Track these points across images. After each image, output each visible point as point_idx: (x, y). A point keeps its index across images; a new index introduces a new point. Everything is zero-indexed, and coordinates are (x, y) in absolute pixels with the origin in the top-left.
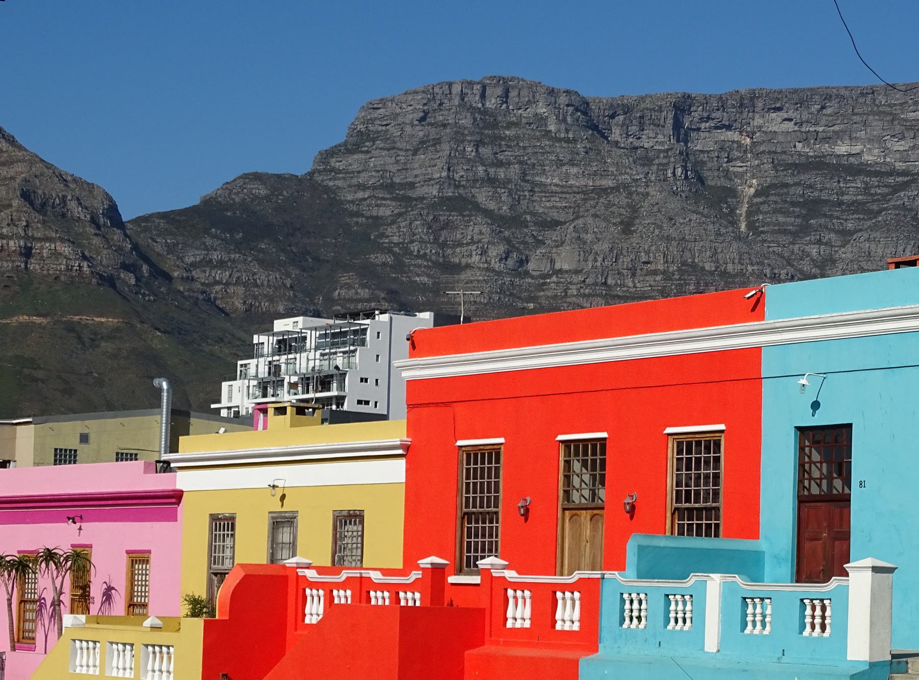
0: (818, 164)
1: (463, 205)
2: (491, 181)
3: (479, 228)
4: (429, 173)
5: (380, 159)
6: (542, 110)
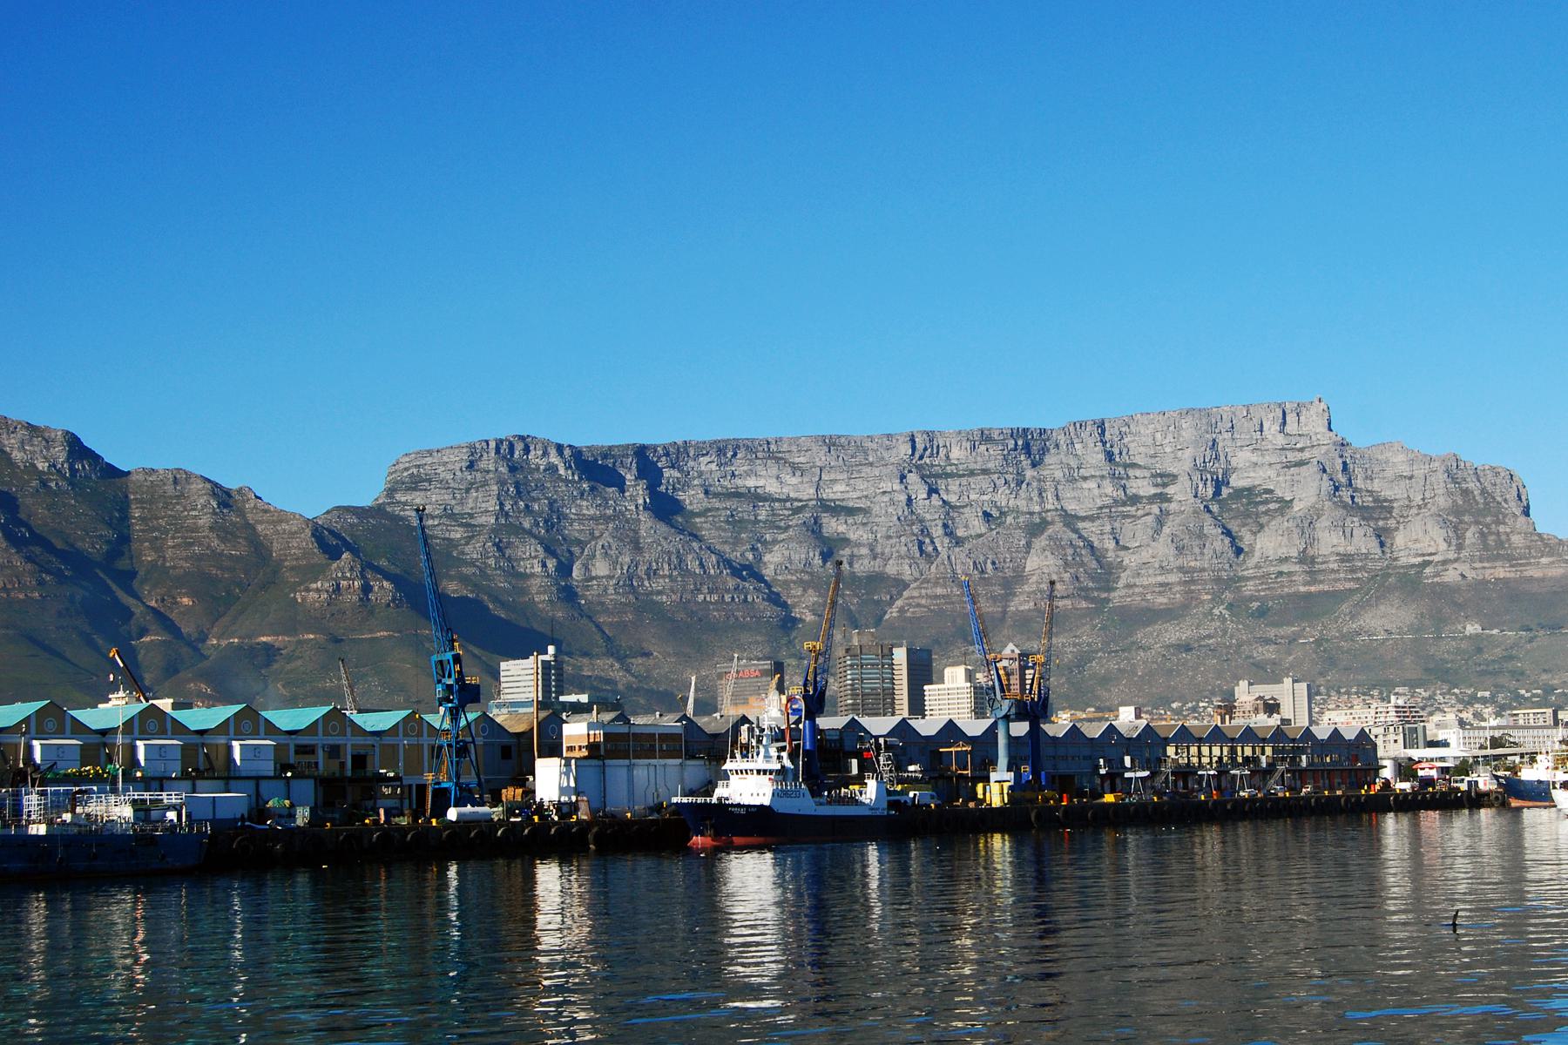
0: (737, 495)
1: (518, 530)
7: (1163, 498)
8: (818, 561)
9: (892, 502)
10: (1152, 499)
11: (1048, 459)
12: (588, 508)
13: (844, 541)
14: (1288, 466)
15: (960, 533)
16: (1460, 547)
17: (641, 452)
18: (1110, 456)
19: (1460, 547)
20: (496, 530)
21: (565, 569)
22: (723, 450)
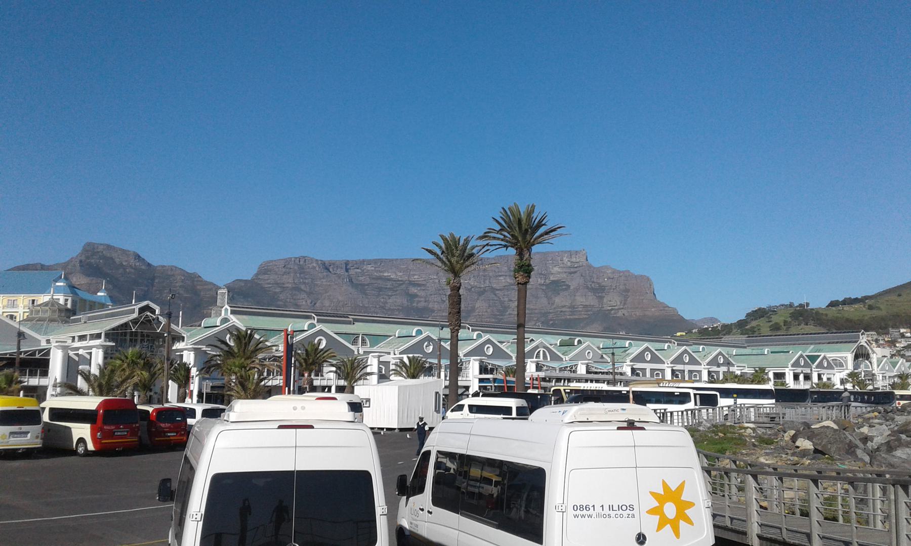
0: (380, 278)
2: (304, 283)
8: (405, 302)
9: (434, 283)
13: (416, 296)
14: (571, 273)
16: (625, 304)
17: (347, 263)
19: (625, 304)
22: (378, 262)
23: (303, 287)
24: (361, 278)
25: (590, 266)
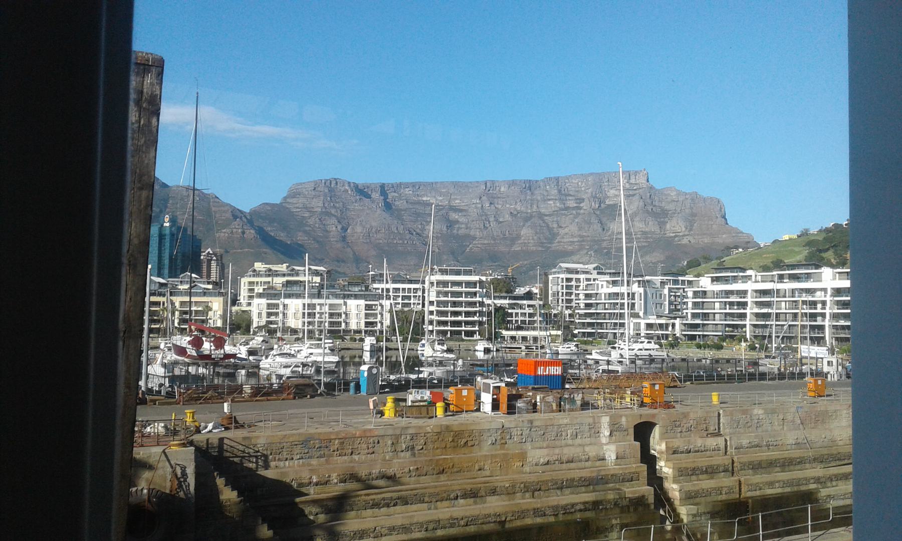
0: (419, 203)
1: (328, 214)
3: (334, 221)
4: (317, 205)
5: (302, 200)
6: (347, 188)
7: (579, 208)
8: (445, 229)
9: (476, 208)
10: (574, 208)
11: (536, 192)
12: (357, 206)
13: (457, 222)
15: (501, 220)
16: (691, 230)
17: (382, 186)
18: (560, 191)
20: (322, 213)
21: (345, 229)
23: (333, 211)
24: (397, 203)
25: (652, 188)
